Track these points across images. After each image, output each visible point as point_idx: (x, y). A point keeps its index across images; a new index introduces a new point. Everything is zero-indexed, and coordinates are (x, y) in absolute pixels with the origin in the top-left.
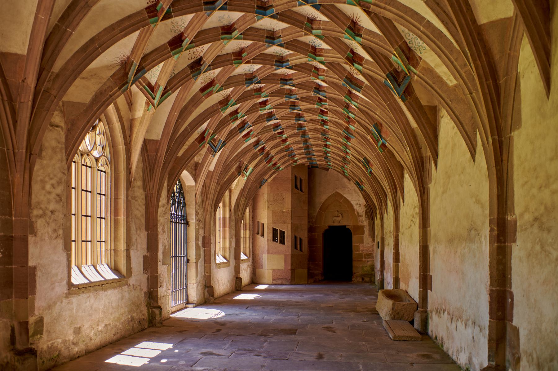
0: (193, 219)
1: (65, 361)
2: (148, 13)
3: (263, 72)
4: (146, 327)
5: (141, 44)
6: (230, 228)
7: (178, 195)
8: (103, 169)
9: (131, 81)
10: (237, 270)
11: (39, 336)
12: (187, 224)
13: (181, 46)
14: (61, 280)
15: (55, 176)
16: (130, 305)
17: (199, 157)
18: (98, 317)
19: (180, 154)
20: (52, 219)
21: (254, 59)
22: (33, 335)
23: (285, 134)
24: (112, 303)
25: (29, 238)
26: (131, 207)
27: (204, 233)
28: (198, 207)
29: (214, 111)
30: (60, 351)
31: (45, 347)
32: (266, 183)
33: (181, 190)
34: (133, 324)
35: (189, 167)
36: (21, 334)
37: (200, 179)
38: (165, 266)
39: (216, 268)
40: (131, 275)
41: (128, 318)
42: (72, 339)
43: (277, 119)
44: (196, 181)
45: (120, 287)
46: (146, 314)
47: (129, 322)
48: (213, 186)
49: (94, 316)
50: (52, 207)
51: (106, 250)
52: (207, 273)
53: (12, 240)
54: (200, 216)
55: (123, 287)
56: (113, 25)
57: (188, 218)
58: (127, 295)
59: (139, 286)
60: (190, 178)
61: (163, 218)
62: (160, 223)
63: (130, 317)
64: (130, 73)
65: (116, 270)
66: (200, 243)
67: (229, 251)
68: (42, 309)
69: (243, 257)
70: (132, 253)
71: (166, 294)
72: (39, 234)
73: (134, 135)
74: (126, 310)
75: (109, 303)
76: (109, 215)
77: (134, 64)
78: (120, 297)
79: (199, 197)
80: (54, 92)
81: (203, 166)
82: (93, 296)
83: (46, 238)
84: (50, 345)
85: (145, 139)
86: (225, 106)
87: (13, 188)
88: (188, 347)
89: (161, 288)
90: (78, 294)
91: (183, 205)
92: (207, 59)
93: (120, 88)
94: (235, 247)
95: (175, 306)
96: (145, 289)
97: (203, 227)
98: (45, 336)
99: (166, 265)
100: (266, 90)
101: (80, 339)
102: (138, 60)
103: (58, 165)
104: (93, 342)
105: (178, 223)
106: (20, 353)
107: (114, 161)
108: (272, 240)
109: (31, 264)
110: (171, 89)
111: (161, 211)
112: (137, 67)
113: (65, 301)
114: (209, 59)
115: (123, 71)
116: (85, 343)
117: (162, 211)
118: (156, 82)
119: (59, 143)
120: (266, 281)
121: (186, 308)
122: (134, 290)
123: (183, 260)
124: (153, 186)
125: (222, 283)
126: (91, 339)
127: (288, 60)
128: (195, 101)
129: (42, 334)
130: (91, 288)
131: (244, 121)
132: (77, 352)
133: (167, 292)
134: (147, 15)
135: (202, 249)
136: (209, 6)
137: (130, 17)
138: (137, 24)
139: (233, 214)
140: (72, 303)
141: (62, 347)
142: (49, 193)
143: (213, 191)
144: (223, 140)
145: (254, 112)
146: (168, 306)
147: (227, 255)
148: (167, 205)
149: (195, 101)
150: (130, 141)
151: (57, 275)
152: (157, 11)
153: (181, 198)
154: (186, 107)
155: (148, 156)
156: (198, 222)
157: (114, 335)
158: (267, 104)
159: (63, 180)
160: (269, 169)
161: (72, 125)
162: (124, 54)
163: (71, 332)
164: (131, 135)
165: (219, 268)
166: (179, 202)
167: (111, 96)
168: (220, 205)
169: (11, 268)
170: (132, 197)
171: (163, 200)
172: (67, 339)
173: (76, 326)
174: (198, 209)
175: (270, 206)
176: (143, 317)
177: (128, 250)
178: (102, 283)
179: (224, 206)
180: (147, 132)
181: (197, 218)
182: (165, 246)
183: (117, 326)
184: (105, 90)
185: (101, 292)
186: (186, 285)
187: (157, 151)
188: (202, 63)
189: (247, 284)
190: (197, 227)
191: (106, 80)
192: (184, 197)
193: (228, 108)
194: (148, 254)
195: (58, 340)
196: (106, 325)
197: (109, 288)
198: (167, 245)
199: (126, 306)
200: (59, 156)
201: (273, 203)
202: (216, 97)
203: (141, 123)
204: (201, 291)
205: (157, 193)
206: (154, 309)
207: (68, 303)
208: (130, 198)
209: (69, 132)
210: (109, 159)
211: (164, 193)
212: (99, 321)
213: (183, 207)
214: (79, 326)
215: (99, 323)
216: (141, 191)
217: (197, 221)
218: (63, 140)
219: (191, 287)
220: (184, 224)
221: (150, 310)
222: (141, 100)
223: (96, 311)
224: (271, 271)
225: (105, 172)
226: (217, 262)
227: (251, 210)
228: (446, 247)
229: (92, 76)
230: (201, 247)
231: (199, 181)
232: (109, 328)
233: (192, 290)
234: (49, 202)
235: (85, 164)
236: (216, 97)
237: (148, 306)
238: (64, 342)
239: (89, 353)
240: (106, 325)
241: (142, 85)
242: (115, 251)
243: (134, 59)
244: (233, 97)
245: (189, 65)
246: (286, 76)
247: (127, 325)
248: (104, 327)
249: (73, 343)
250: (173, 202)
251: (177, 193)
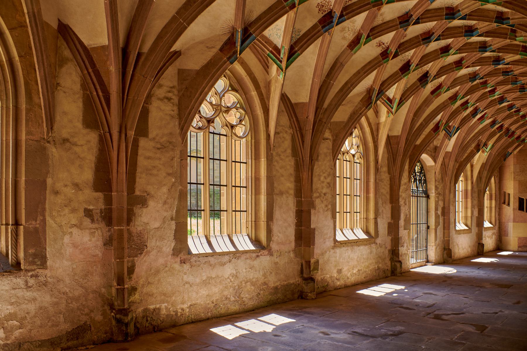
0: (432, 193)
1: (332, 289)
2: (382, 57)
3: (484, 70)
4: (389, 275)
5: (379, 76)
6: (472, 199)
7: (419, 174)
8: (358, 161)
9: (374, 102)
10: (480, 236)
11: (316, 271)
12: (428, 197)
13: (409, 69)
14: (330, 237)
15: (326, 171)
16: (377, 258)
17: (438, 142)
18: (353, 264)
19: (418, 142)
20: (325, 198)
21: (473, 63)
22: (313, 270)
23: (522, 111)
24: (363, 255)
25: (312, 211)
26: (378, 187)
27: (444, 204)
28: (437, 183)
29: (445, 106)
30: (328, 282)
31: (319, 278)
32: (512, 155)
33: (421, 171)
34: (379, 272)
35: (429, 150)
36: (306, 268)
37: (439, 159)
38: (406, 231)
39: (456, 234)
40: (378, 237)
41: (375, 268)
42: (336, 276)
43: (509, 101)
44: (435, 161)
45: (369, 244)
46: (390, 266)
47: (376, 270)
48: (451, 164)
49: (350, 263)
50: (324, 191)
51: (360, 218)
52: (446, 237)
53: (302, 212)
54: (439, 190)
55: (372, 245)
56: (359, 70)
57: (429, 192)
58: (374, 250)
59: (384, 245)
60: (430, 159)
61: (405, 193)
62: (402, 198)
63: (376, 267)
64: (373, 97)
65: (367, 232)
66: (439, 212)
67: (471, 219)
68: (318, 255)
69: (487, 224)
70: (379, 220)
71: (406, 252)
72: (317, 208)
73: (380, 135)
74: (374, 261)
75: (361, 255)
76: (362, 193)
77: (375, 90)
78: (369, 251)
79: (439, 174)
80: (324, 120)
81: (441, 149)
82: (350, 249)
83: (321, 211)
84: (322, 278)
85: (388, 135)
86: (454, 100)
87: (303, 182)
88: (416, 289)
89: (402, 247)
90: (340, 247)
91: (424, 181)
92: (432, 72)
93: (366, 108)
94: (477, 215)
95: (416, 263)
96: (389, 247)
97: (443, 199)
98: (319, 272)
99: (407, 230)
100: (491, 82)
101: (341, 277)
102: (378, 87)
103: (328, 164)
104: (349, 280)
105: (419, 197)
106: (305, 279)
107: (365, 156)
108: (518, 209)
109: (312, 227)
110: (405, 99)
112: (377, 92)
113: (332, 251)
114: (434, 72)
115: (368, 96)
116: (344, 280)
117: (404, 188)
118: (393, 96)
119: (328, 149)
120: (511, 248)
121: (425, 265)
122: (380, 247)
123: (424, 227)
124: (396, 170)
125: (462, 247)
126: (348, 278)
127: (504, 59)
128: (427, 102)
129: (318, 270)
130: (349, 244)
131: (476, 107)
132: (339, 285)
133: (407, 251)
134: (381, 58)
135: (441, 217)
136: (426, 41)
137: (370, 62)
138: (375, 65)
139: (475, 187)
140: (336, 253)
141: (330, 280)
142: (323, 182)
143: (451, 168)
144: (456, 126)
145: (484, 100)
146: (408, 262)
147: (469, 223)
148: (408, 183)
149: (427, 102)
150: (377, 139)
151: (327, 234)
152: (388, 54)
153: (422, 176)
154: (420, 108)
155: (391, 148)
156: (437, 195)
157: (364, 278)
158: (496, 91)
159: (331, 173)
160: (512, 143)
161: (336, 136)
162: (369, 84)
163: (335, 271)
164: (377, 135)
165: (460, 234)
166: (420, 180)
167: (361, 114)
168: (461, 178)
169: (302, 229)
170: (379, 180)
171: (405, 179)
172: (333, 275)
173: (338, 268)
174: (438, 185)
175: (516, 177)
176: (387, 268)
177: (376, 219)
178: (357, 241)
179: (466, 179)
180: (390, 130)
181: (437, 192)
182: (407, 215)
183: (367, 272)
184: (357, 111)
185: (356, 247)
186: (427, 247)
187: (398, 143)
188: (428, 75)
189: (491, 250)
190: (437, 200)
191: (357, 104)
192: (425, 176)
193: (457, 101)
194: (392, 222)
195: (327, 275)
196: (359, 270)
197: (361, 245)
198: (408, 214)
199: (374, 259)
200: (329, 158)
201: (519, 174)
202: (445, 96)
203: (384, 126)
204: (439, 253)
205: (398, 175)
206: (395, 263)
207: (334, 252)
208: (377, 181)
209: (334, 141)
210: (362, 154)
211: (405, 174)
212: (353, 267)
213: (424, 183)
214: (340, 268)
215: (354, 268)
216: (387, 175)
217: (437, 194)
218: (331, 147)
219: (431, 249)
220: (425, 197)
221: (393, 263)
222: (384, 110)
223: (352, 259)
224: (517, 239)
225: (360, 163)
226: (457, 229)
227: (497, 181)
229: (348, 102)
230: (440, 216)
231: (438, 161)
232: (361, 272)
233: (431, 251)
234: (323, 188)
235: (346, 160)
236: (445, 96)
237: (392, 260)
238: (331, 277)
239: (346, 287)
240: (359, 270)
241: (383, 99)
242: (367, 219)
243: (375, 86)
244: (461, 92)
245: (418, 79)
246: (508, 68)
247: (374, 272)
248: (357, 271)
249: (337, 279)
250: (414, 180)
251: (418, 172)
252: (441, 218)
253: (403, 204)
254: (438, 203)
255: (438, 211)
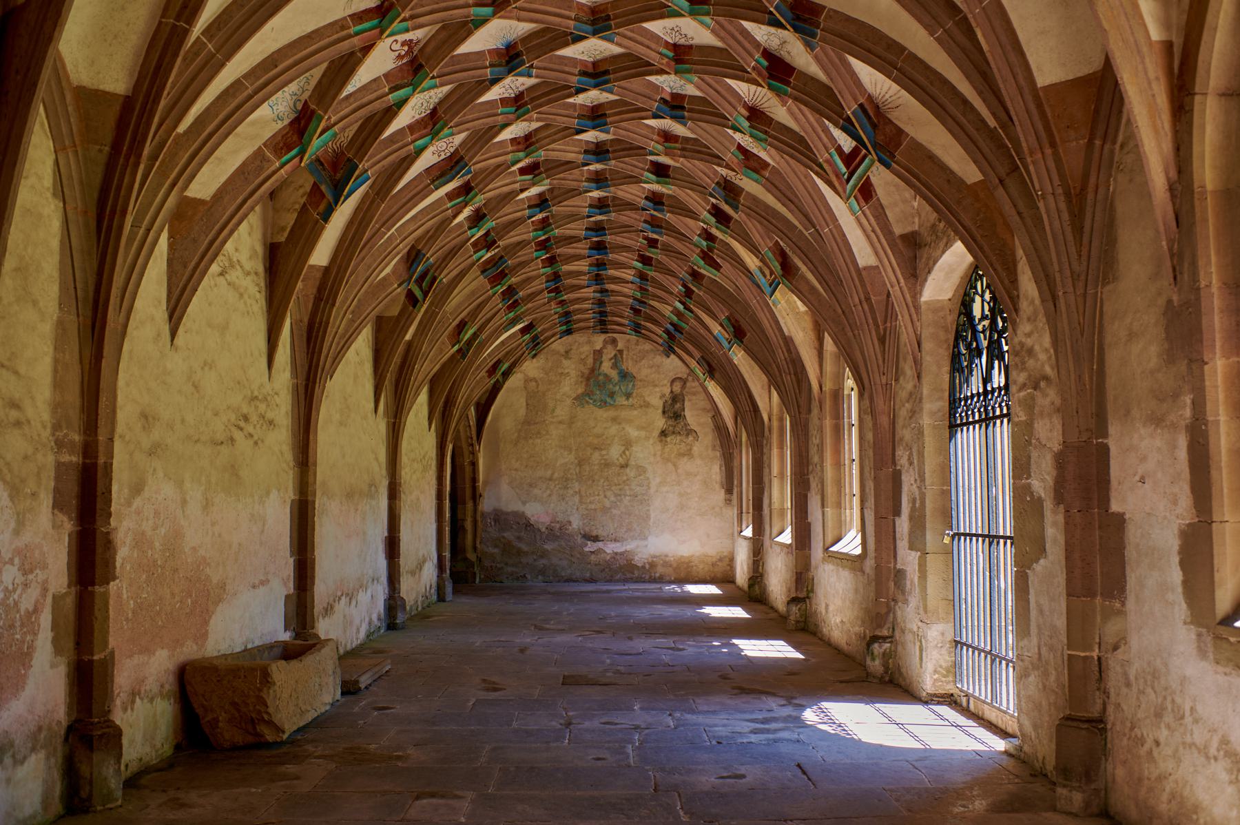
62: (904, 445)
111: (905, 413)
135: (1054, 512)
174: (1029, 335)
228: (341, 503)
230: (1048, 505)
252: (1049, 516)
253: (907, 465)
254: (1031, 434)
255: (1029, 477)
